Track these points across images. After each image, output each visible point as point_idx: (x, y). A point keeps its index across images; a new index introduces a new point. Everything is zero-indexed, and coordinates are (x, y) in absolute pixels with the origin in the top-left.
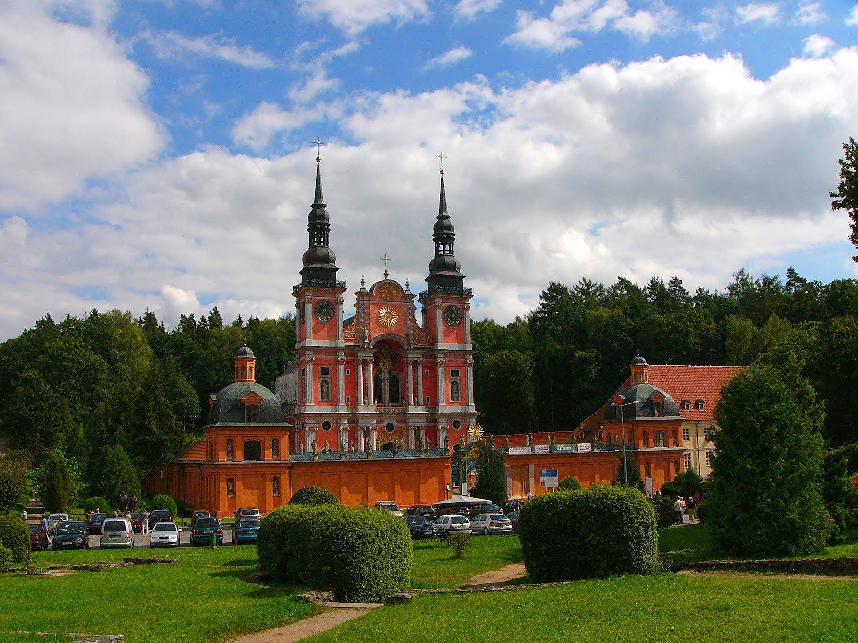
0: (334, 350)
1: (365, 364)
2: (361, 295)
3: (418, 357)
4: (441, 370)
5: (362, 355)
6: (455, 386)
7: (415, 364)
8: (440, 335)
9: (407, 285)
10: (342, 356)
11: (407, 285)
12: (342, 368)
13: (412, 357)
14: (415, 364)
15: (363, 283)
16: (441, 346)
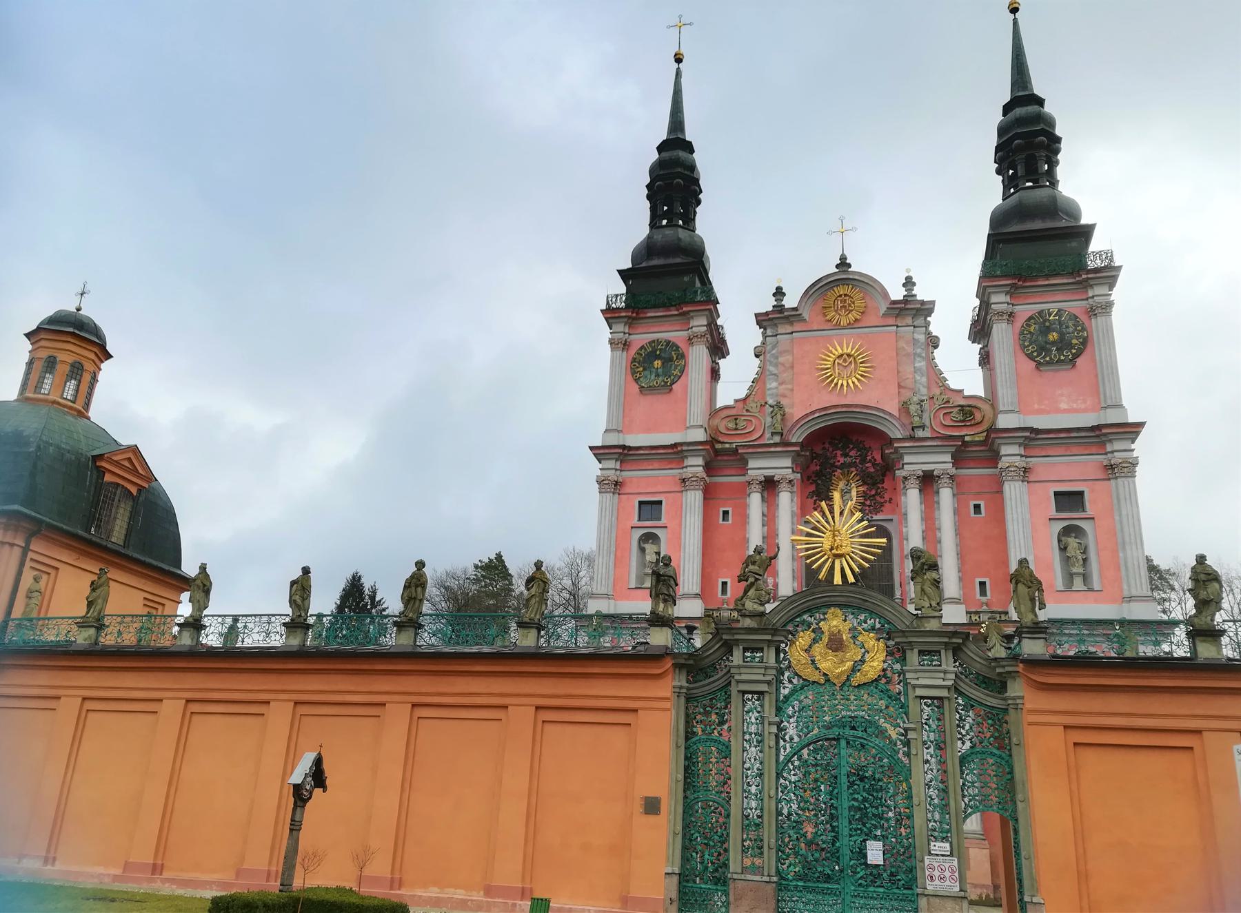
0: (676, 453)
1: (770, 485)
2: (774, 319)
3: (940, 462)
4: (1014, 491)
5: (759, 467)
6: (1072, 542)
7: (928, 481)
8: (1005, 396)
9: (909, 283)
10: (695, 465)
11: (909, 283)
12: (694, 499)
13: (914, 463)
14: (928, 481)
15: (779, 293)
16: (1003, 422)
